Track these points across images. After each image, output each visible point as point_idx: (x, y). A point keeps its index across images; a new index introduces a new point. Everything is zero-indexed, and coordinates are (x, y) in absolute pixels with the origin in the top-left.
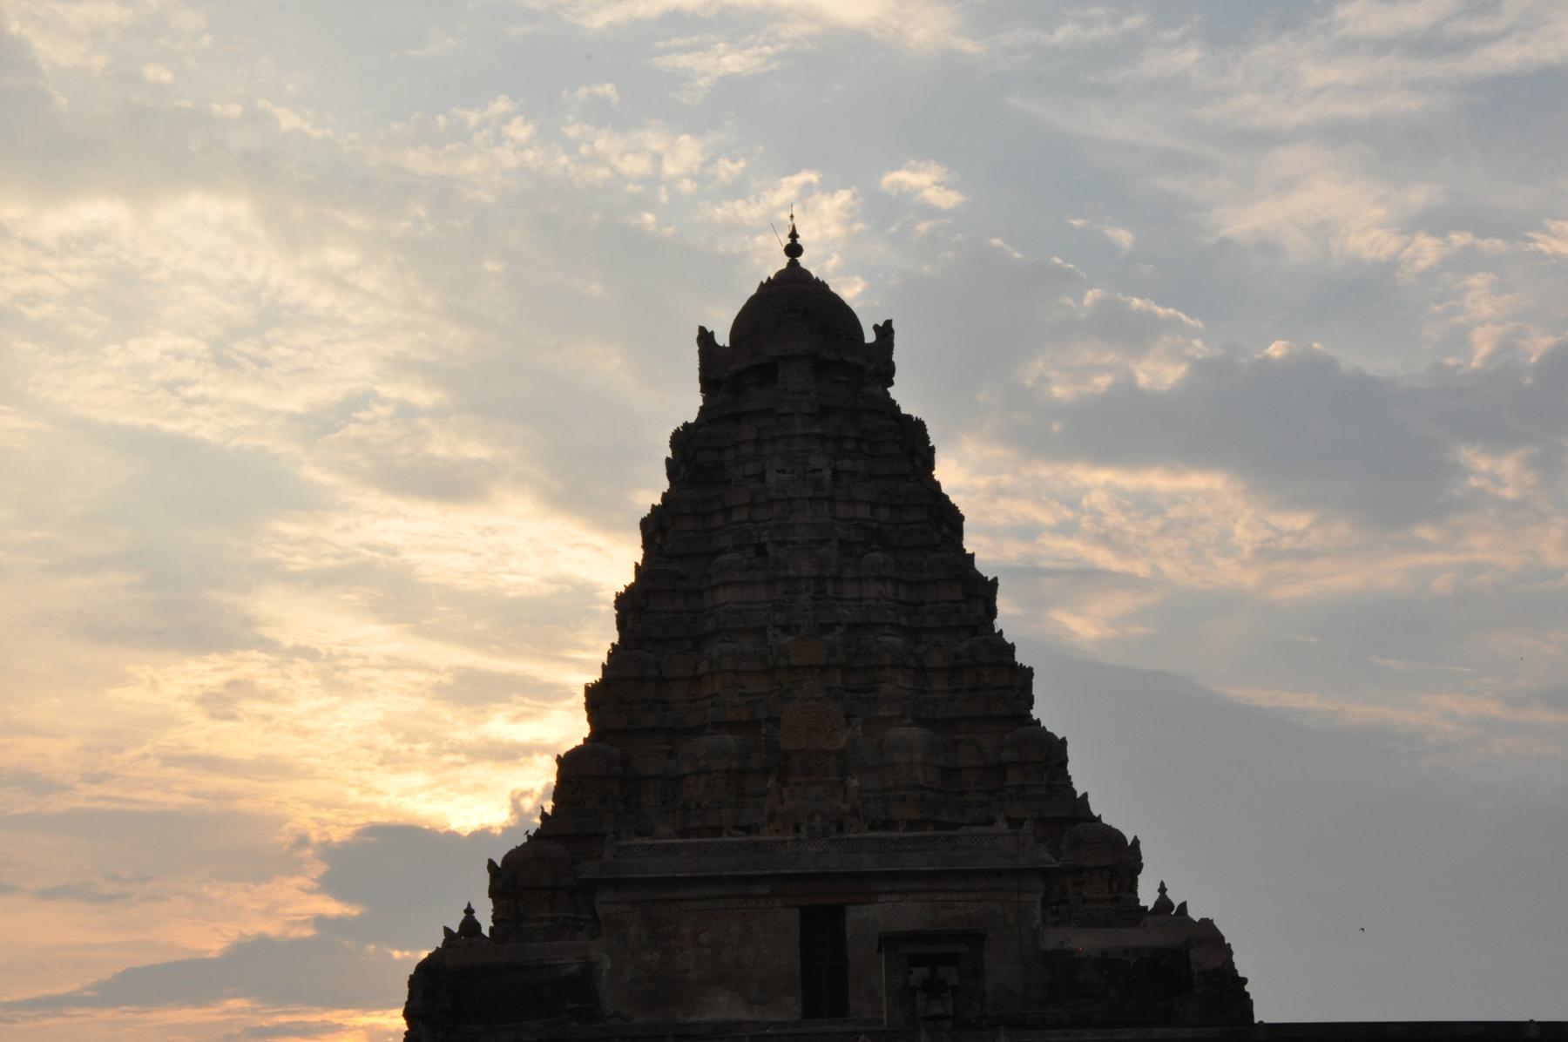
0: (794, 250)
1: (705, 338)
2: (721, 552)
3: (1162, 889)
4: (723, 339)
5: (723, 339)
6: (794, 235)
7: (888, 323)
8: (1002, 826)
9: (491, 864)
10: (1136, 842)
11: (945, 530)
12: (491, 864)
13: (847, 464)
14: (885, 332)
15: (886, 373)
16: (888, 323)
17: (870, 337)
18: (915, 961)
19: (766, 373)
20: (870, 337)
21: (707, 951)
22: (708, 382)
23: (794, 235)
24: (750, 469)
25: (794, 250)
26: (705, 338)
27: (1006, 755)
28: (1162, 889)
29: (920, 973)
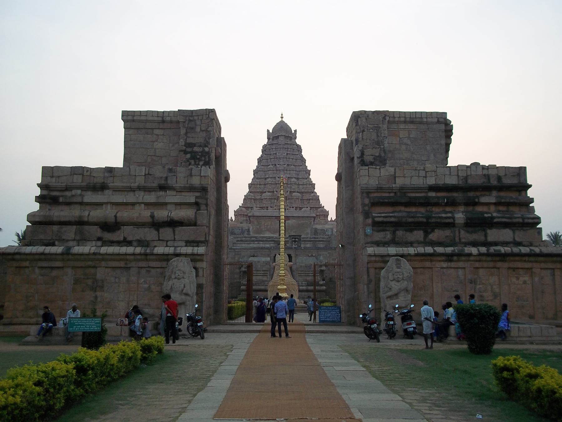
0: (282, 118)
1: (268, 131)
2: (270, 165)
3: (331, 218)
4: (271, 131)
5: (271, 131)
6: (282, 115)
7: (296, 130)
8: (309, 208)
9: (234, 211)
10: (328, 211)
11: (303, 162)
12: (234, 211)
13: (288, 152)
14: (296, 131)
15: (296, 138)
16: (296, 130)
17: (293, 132)
18: (293, 238)
19: (277, 137)
20: (293, 132)
21: (266, 226)
22: (268, 138)
23: (282, 115)
24: (275, 152)
25: (282, 118)
26: (268, 131)
27: (310, 198)
28: (331, 218)
29: (294, 239)
